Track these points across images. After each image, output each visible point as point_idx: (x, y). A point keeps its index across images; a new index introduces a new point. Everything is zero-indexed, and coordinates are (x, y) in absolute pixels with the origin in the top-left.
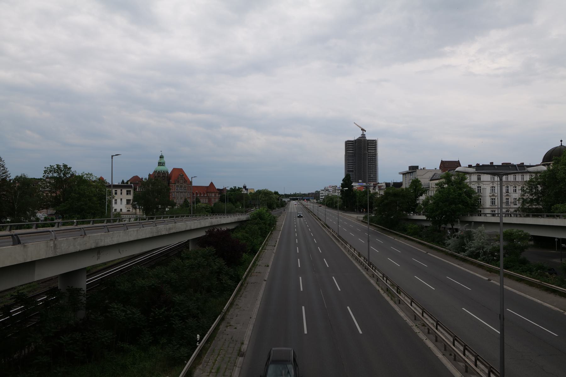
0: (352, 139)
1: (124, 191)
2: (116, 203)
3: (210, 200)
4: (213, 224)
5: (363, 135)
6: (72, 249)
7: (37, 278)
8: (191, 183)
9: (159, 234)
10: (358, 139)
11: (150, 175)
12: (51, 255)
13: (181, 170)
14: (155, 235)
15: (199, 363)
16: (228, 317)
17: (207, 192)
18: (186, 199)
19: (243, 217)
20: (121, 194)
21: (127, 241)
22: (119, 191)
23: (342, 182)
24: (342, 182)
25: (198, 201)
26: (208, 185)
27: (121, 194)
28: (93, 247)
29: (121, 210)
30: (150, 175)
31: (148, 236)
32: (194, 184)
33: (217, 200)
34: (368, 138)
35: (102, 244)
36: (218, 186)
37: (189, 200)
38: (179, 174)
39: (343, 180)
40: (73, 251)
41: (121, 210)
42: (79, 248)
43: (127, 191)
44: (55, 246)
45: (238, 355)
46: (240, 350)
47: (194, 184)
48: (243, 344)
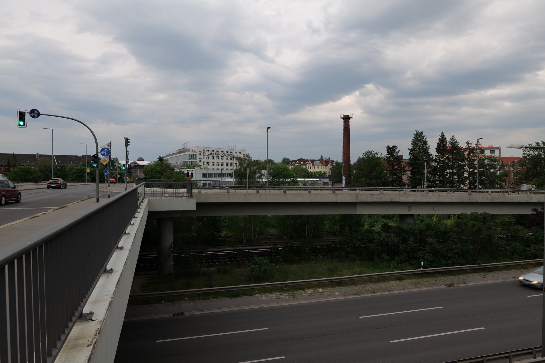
6: (369, 200)
7: (358, 213)
9: (474, 201)
12: (354, 200)
14: (466, 201)
15: (415, 279)
16: (499, 272)
21: (426, 200)
28: (388, 200)
31: (455, 201)
35: (397, 200)
40: (371, 201)
42: (375, 200)
44: (357, 197)
45: (446, 285)
46: (453, 284)
48: (464, 283)
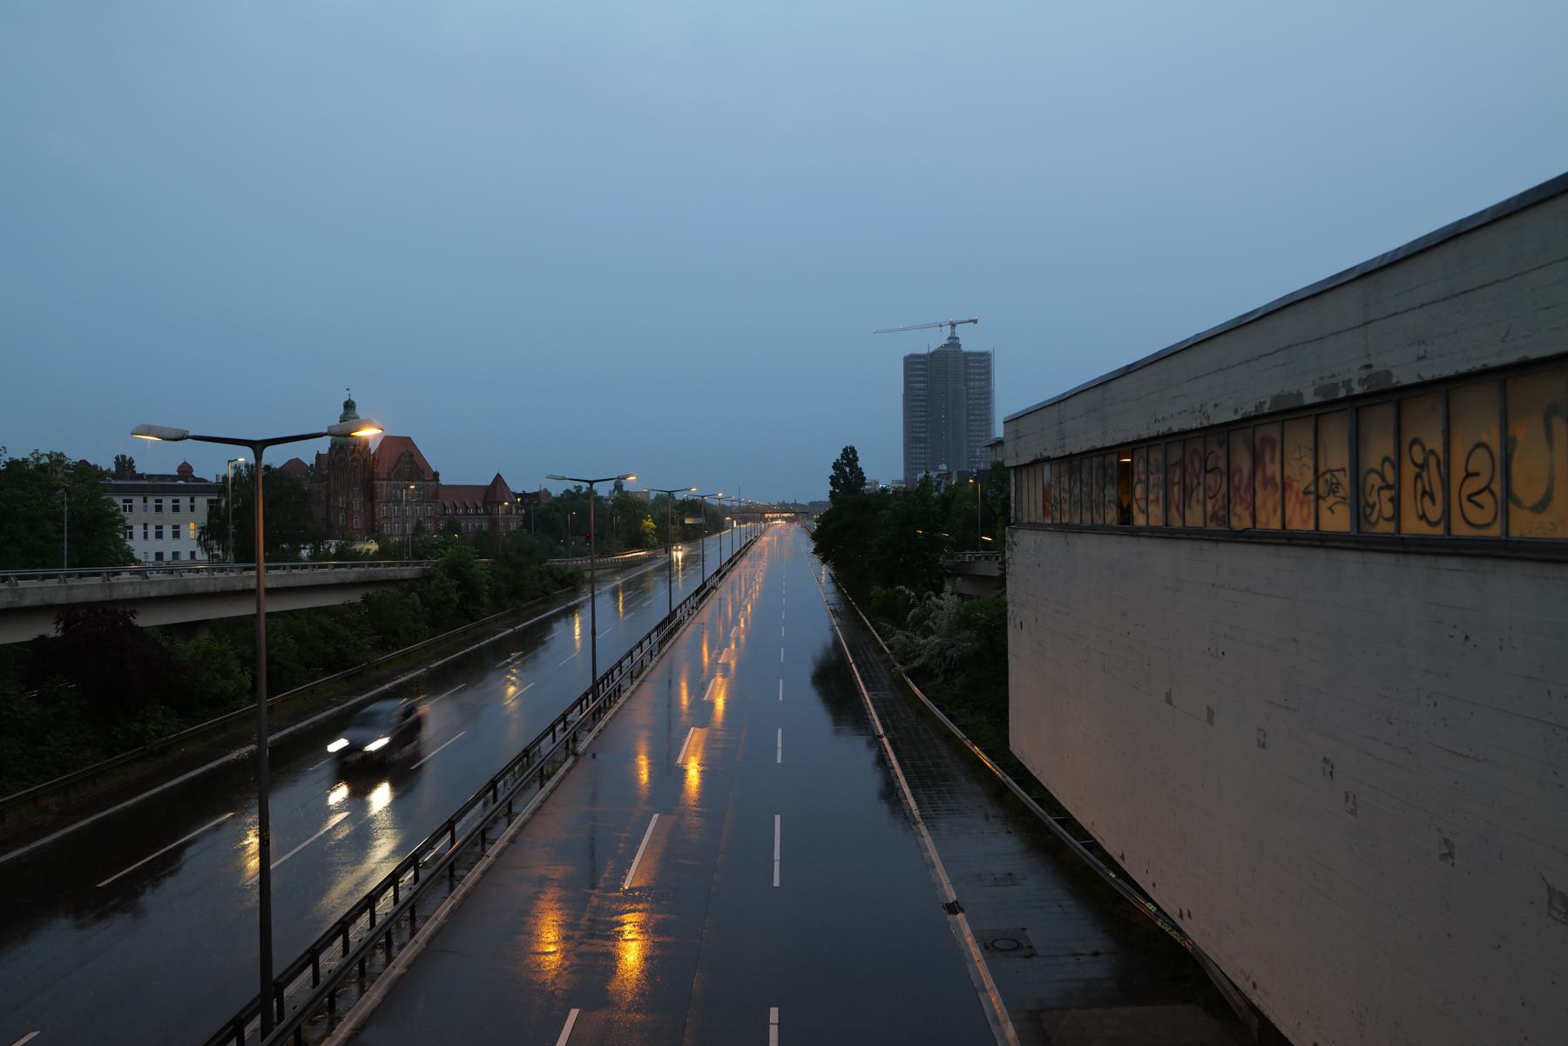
0: (923, 351)
1: (202, 502)
2: (176, 535)
3: (494, 523)
4: (198, 589)
5: (954, 339)
8: (436, 475)
10: (936, 352)
11: (319, 456)
13: (407, 441)
17: (485, 503)
18: (419, 522)
19: (409, 572)
20: (192, 509)
22: (184, 501)
23: (832, 472)
24: (832, 472)
25: (453, 526)
26: (488, 483)
27: (192, 509)
29: (193, 554)
30: (319, 456)
32: (443, 481)
33: (513, 526)
34: (965, 348)
36: (517, 485)
37: (429, 525)
38: (403, 457)
39: (836, 466)
41: (193, 554)
43: (210, 501)
47: (443, 481)
